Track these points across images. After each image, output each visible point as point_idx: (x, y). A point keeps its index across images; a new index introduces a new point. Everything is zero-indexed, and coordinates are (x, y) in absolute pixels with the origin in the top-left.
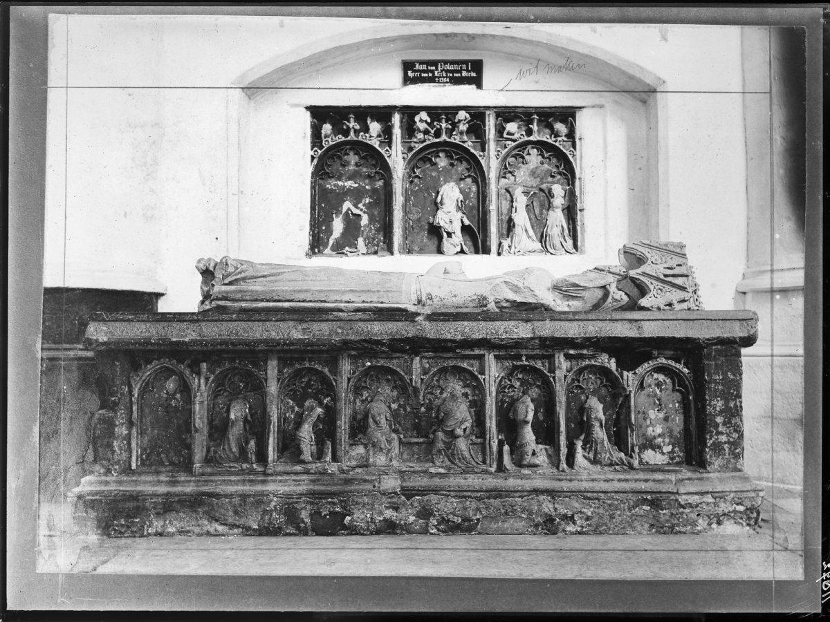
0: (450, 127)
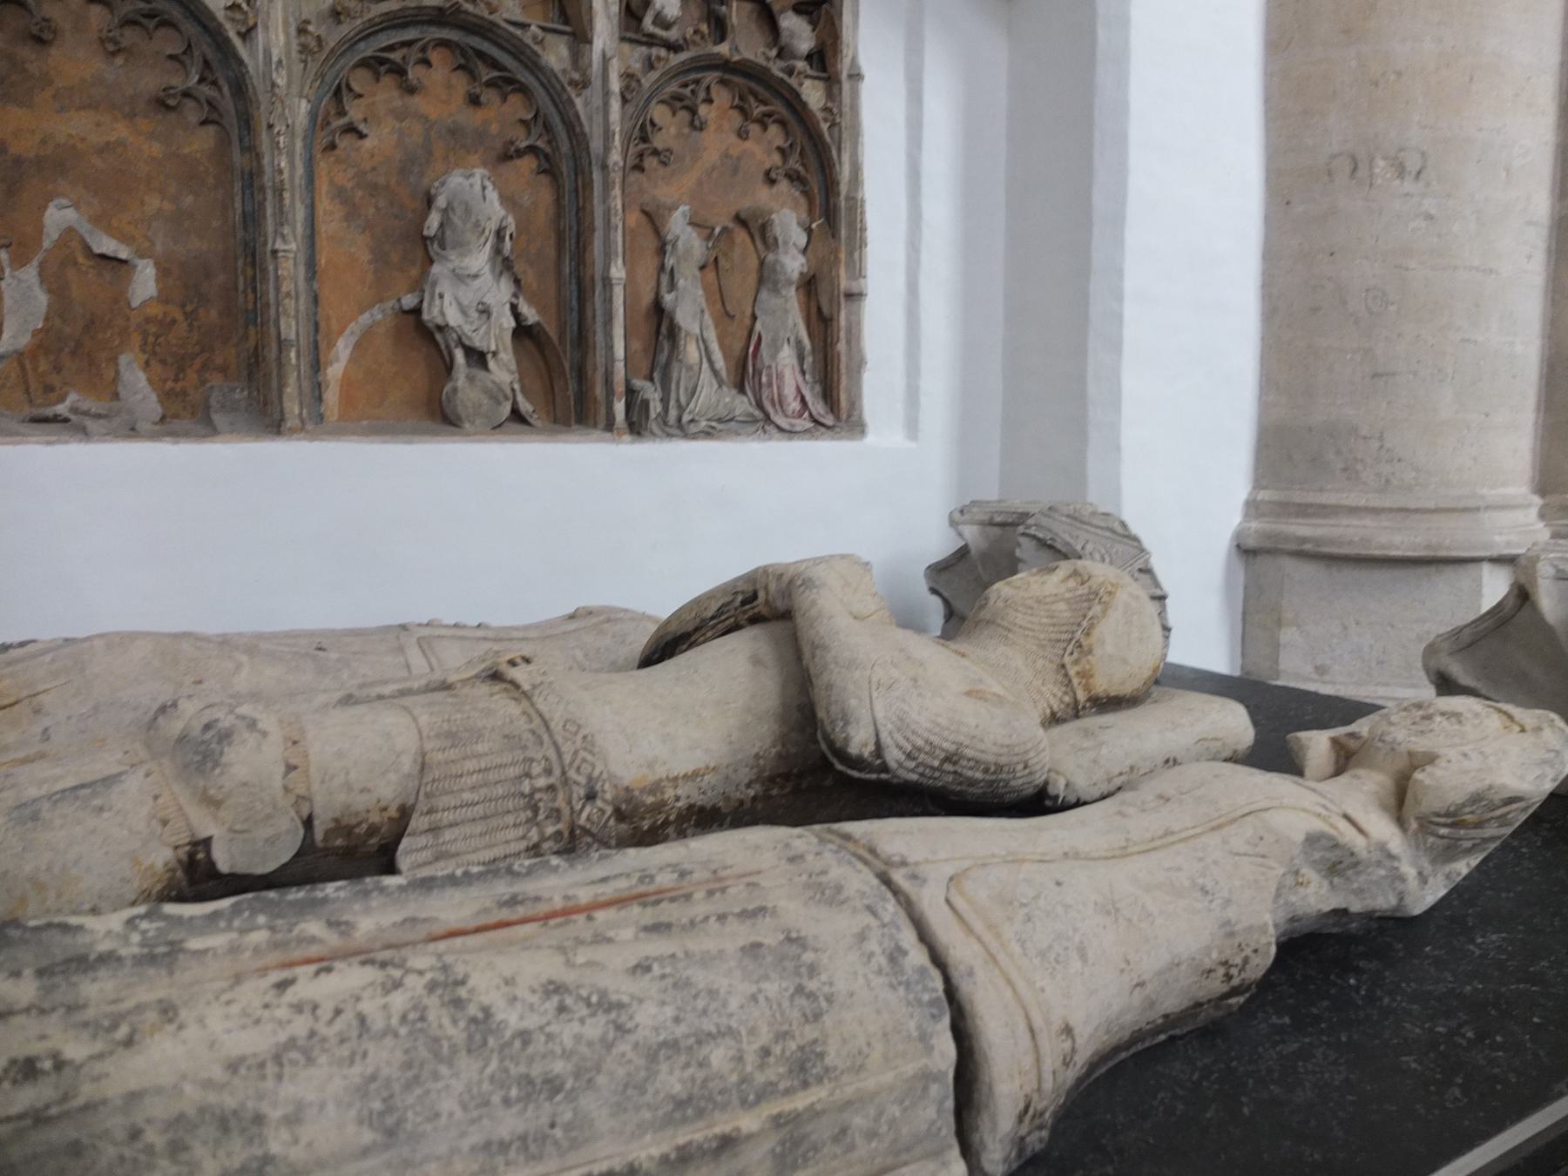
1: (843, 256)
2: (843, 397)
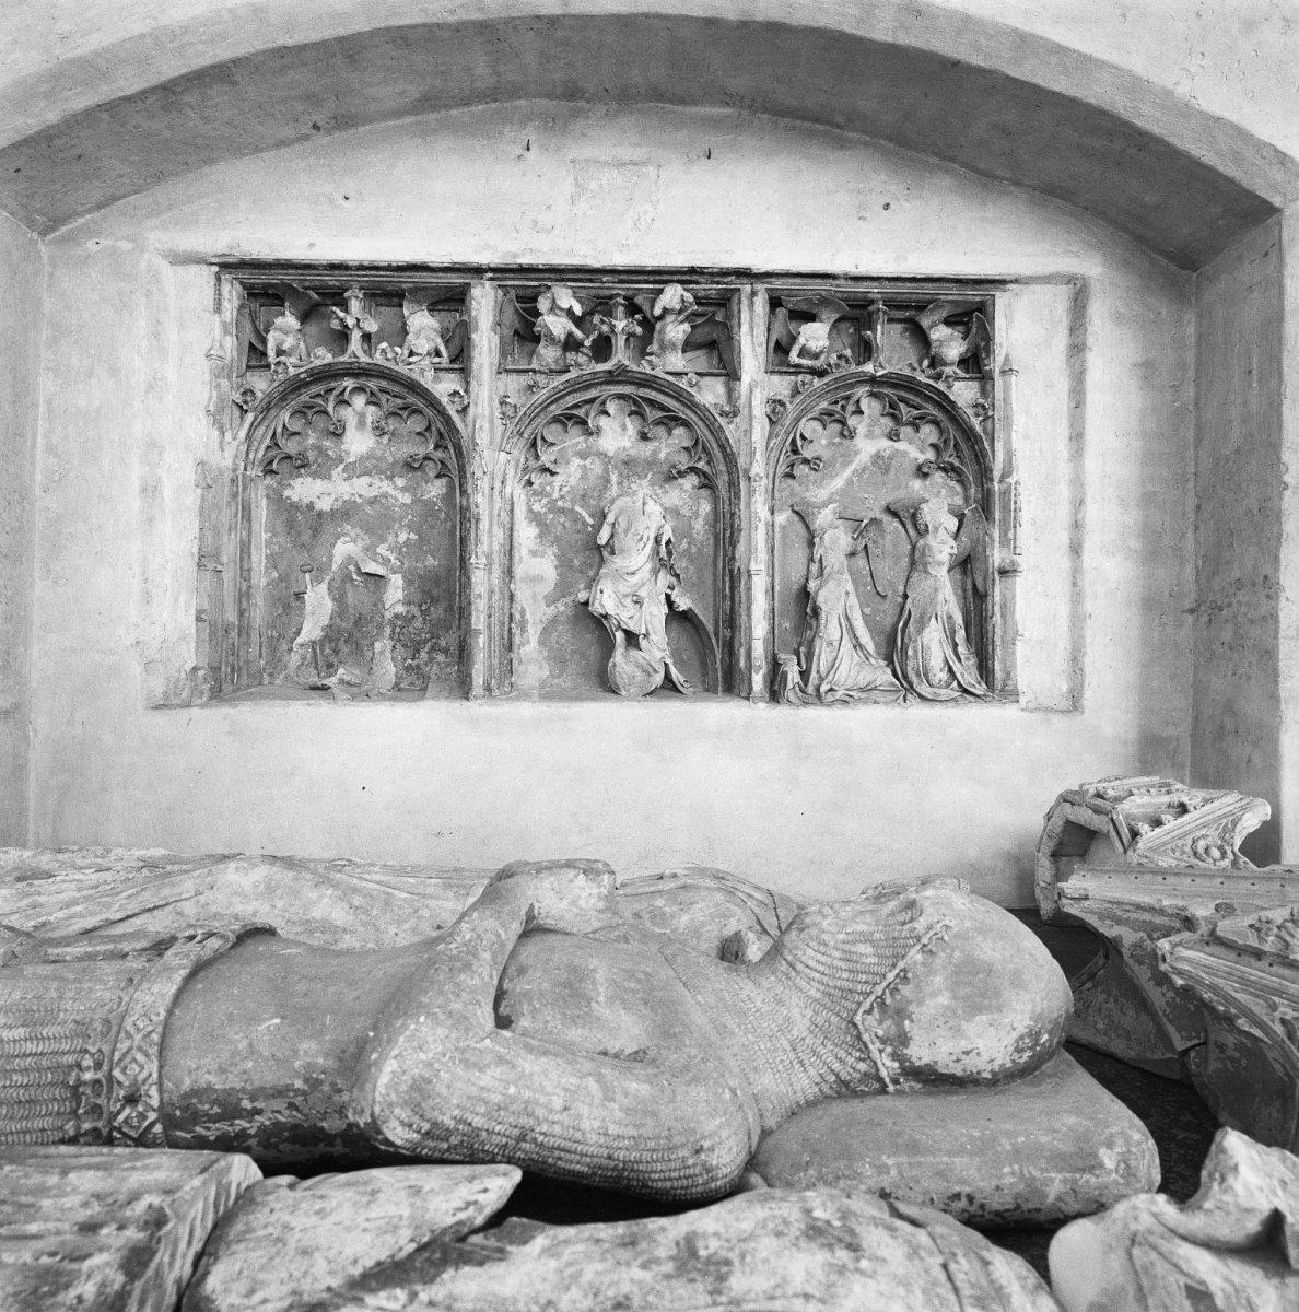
0: (639, 330)
1: (996, 534)
2: (998, 667)
